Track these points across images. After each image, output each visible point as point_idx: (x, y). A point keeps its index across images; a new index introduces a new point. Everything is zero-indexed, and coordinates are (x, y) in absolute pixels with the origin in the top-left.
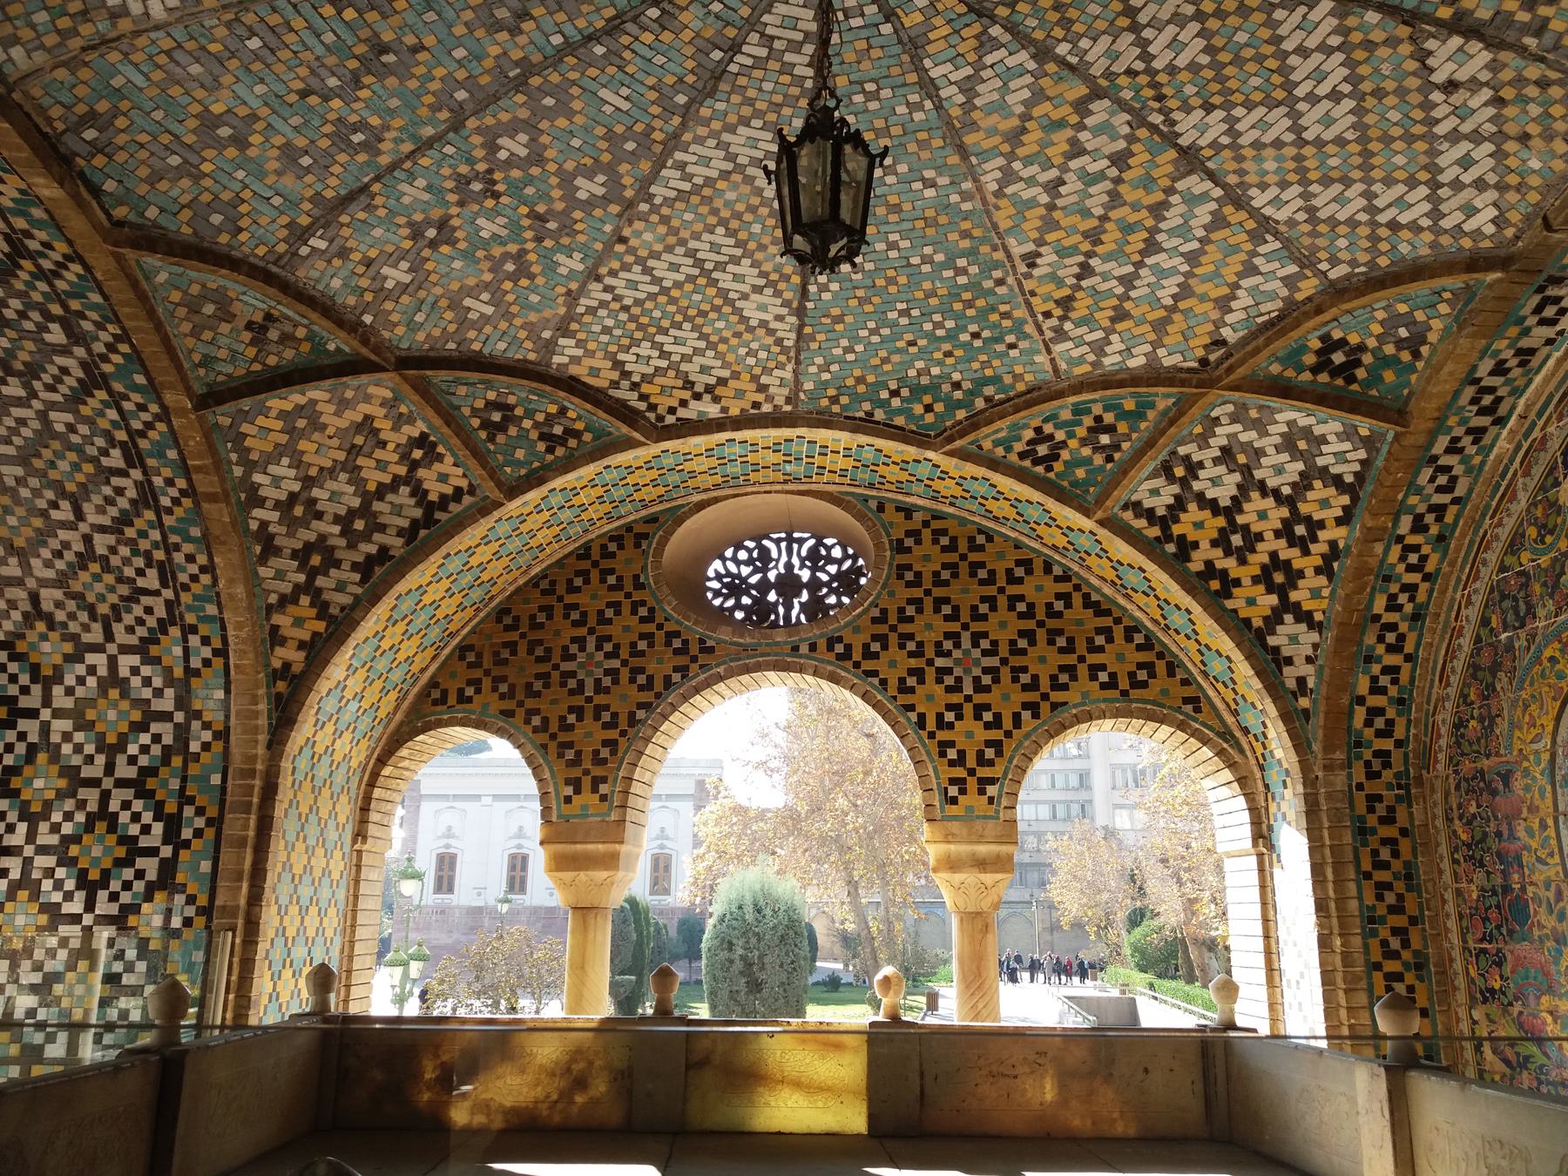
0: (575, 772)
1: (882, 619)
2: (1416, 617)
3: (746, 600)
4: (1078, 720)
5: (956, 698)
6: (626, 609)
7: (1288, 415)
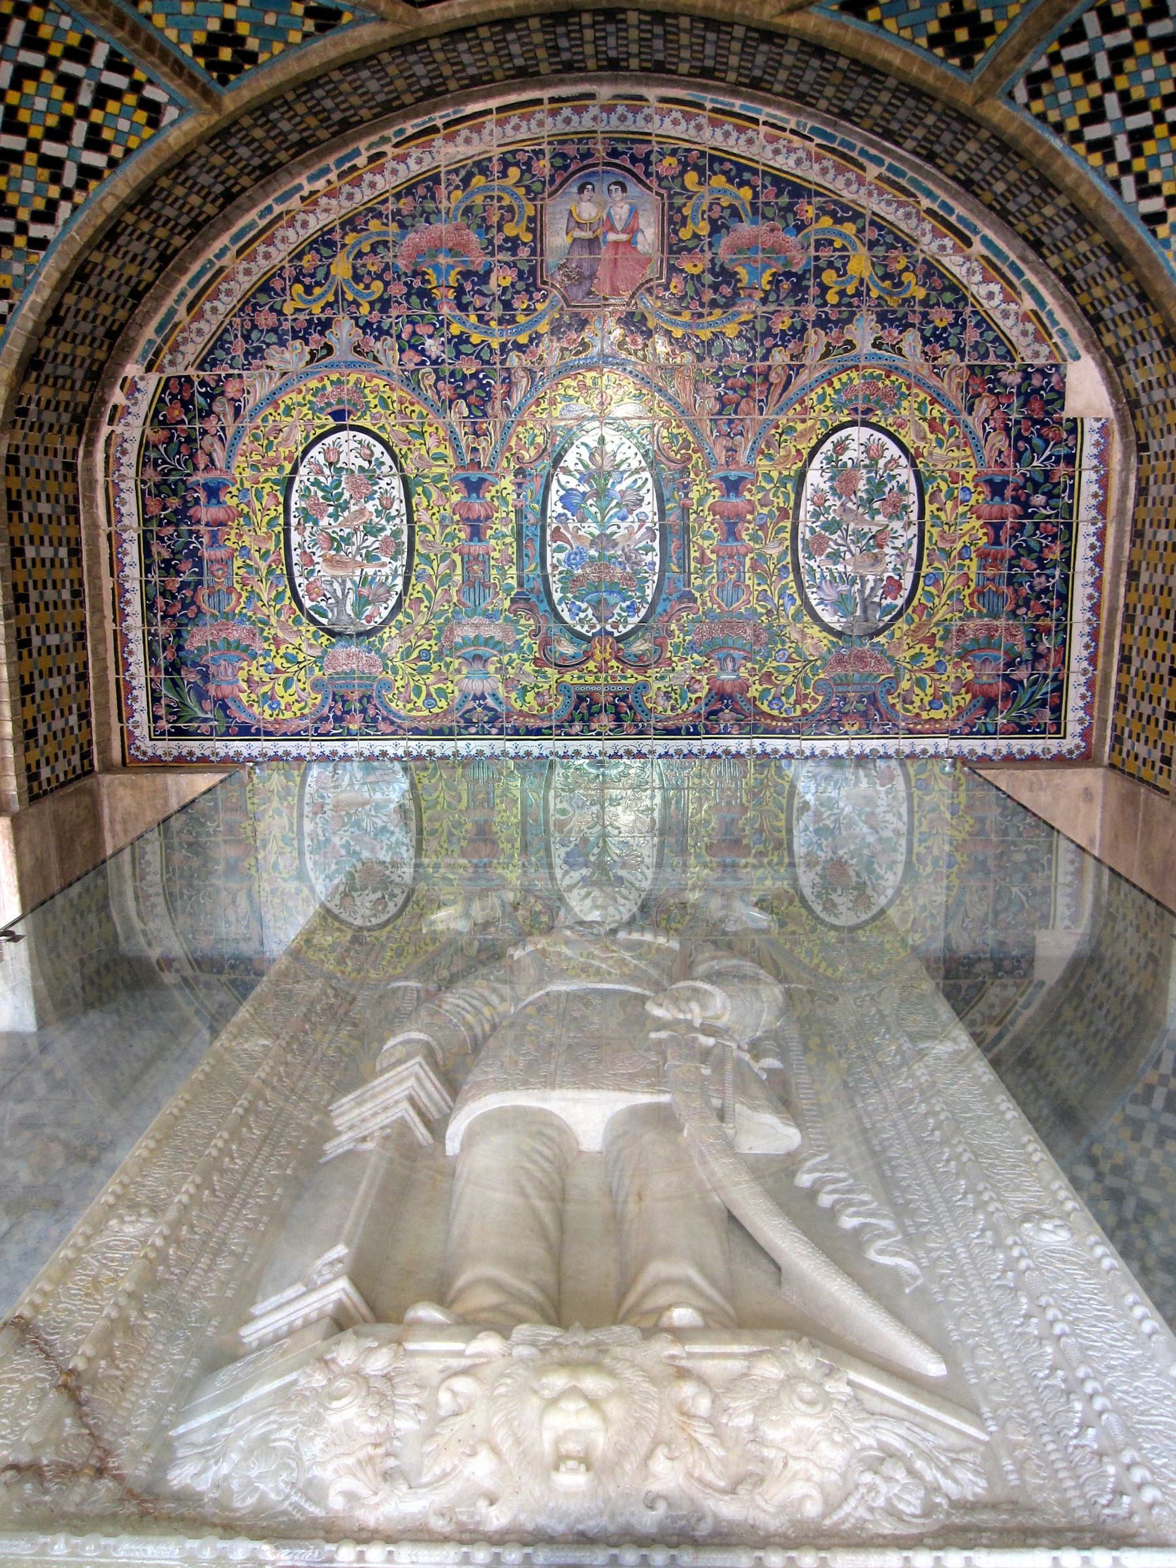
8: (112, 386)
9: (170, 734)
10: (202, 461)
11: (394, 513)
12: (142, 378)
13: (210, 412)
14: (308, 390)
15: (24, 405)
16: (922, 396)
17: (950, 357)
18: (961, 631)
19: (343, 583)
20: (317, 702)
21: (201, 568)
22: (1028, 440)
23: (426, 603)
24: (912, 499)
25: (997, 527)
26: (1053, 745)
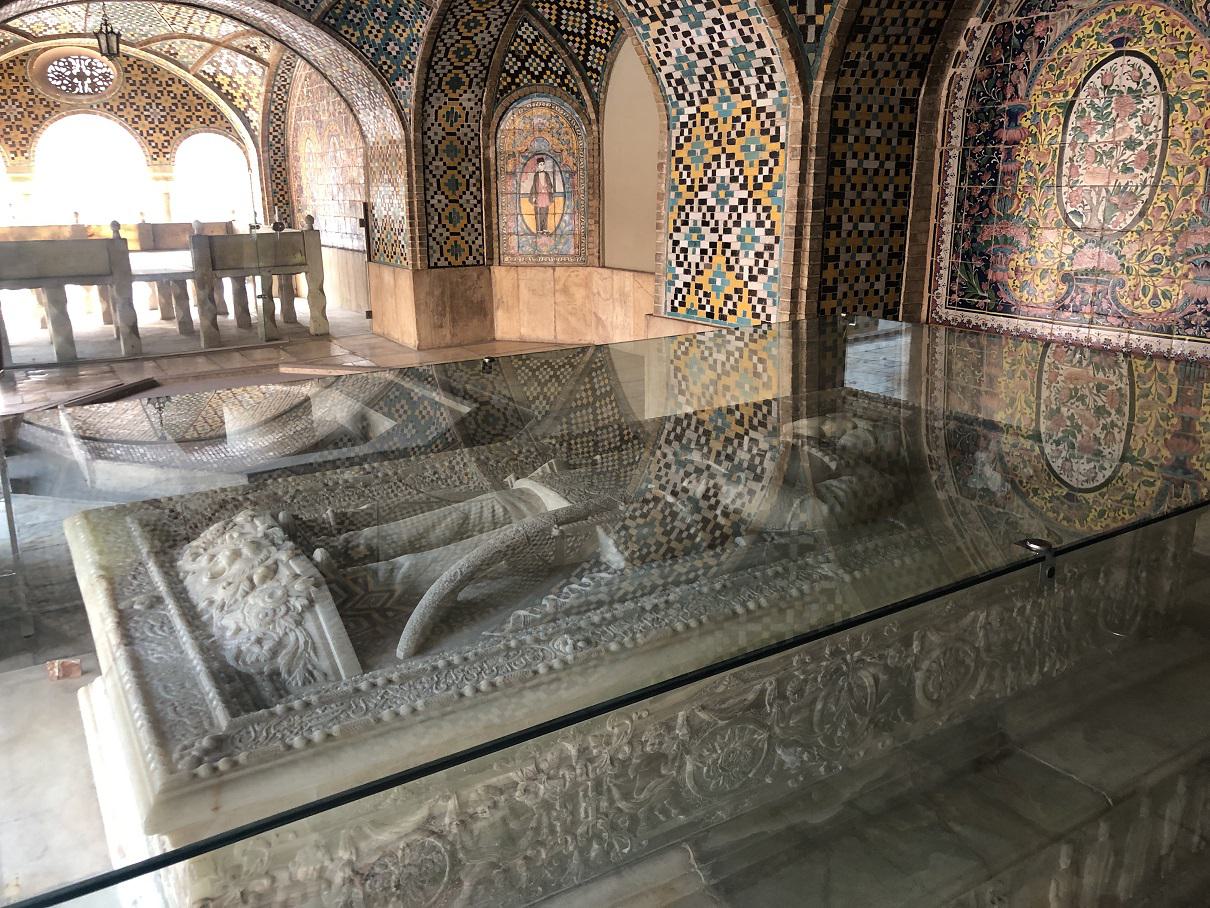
0: (13, 149)
1: (122, 97)
2: (283, 112)
3: (65, 82)
4: (193, 133)
5: (152, 126)
6: (22, 89)
7: (241, 57)
8: (958, 37)
9: (959, 305)
10: (1009, 92)
11: (1152, 129)
12: (979, 28)
13: (1021, 50)
14: (1096, 24)
15: (852, 58)
19: (1098, 194)
20: (1063, 292)
21: (996, 177)
23: (1167, 212)
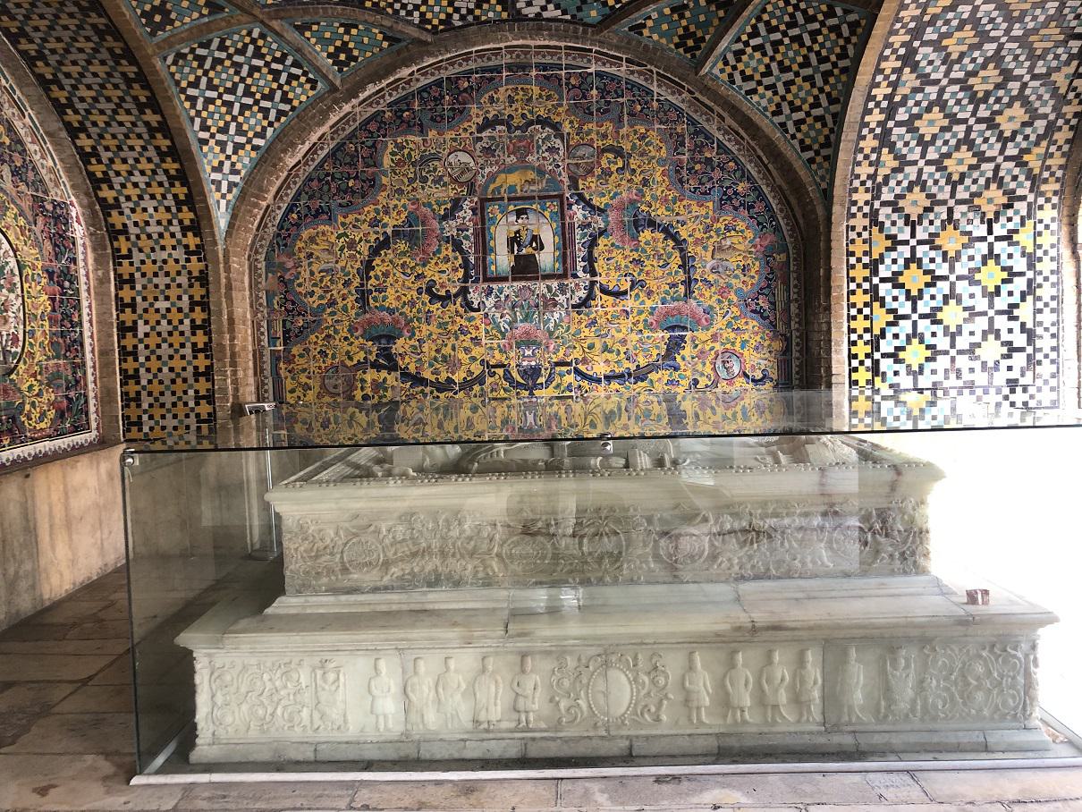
16: (15, 210)
17: (23, 187)
18: (46, 368)
22: (59, 247)
24: (17, 279)
25: (53, 300)
26: (79, 439)
